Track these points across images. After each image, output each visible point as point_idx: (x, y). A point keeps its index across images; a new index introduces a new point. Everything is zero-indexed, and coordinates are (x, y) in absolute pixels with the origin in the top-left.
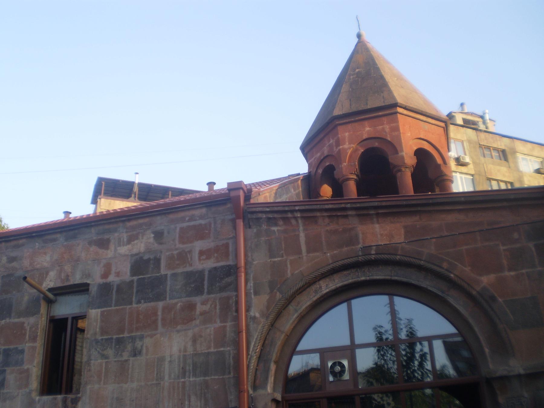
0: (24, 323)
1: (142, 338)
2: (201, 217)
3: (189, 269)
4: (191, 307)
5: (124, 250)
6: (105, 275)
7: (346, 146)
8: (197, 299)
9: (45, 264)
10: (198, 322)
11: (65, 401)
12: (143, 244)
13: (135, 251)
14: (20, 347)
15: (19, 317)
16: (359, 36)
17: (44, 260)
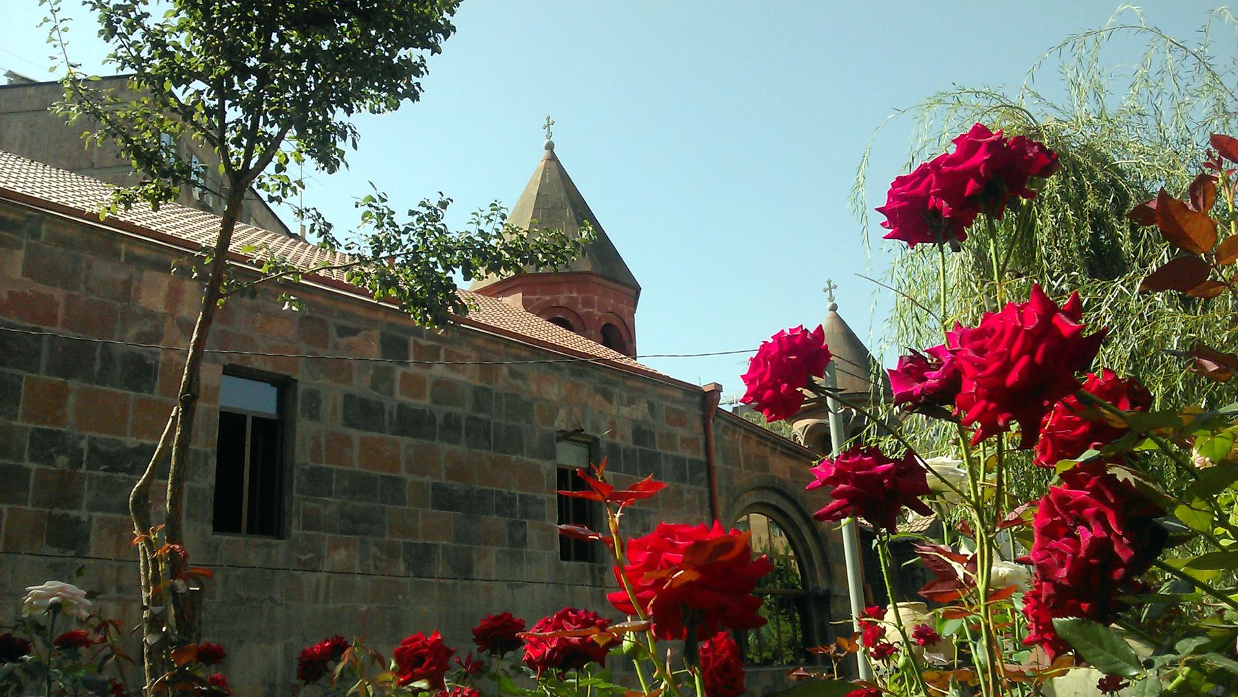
0: (539, 466)
1: (649, 514)
2: (681, 402)
3: (674, 453)
4: (679, 492)
5: (625, 411)
6: (612, 435)
7: (595, 311)
8: (685, 487)
9: (554, 398)
10: (685, 508)
11: (592, 570)
12: (639, 411)
13: (634, 417)
14: (539, 496)
15: (533, 457)
16: (550, 147)
17: (553, 391)
